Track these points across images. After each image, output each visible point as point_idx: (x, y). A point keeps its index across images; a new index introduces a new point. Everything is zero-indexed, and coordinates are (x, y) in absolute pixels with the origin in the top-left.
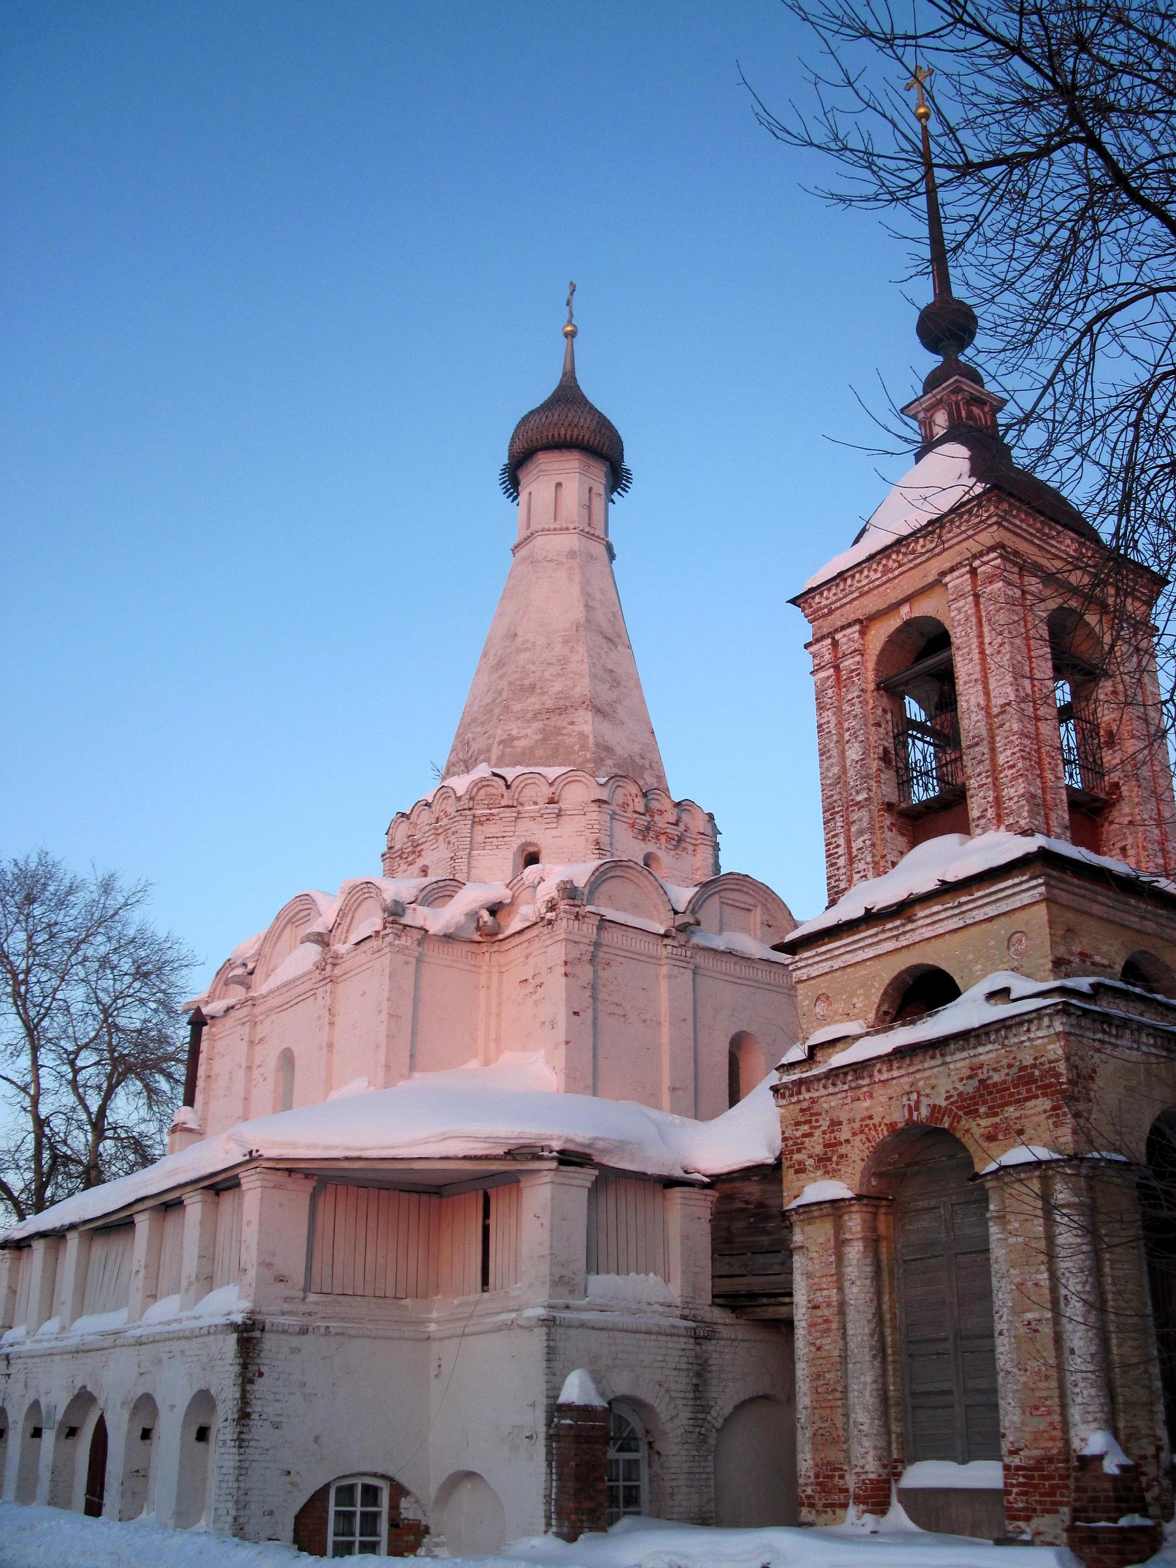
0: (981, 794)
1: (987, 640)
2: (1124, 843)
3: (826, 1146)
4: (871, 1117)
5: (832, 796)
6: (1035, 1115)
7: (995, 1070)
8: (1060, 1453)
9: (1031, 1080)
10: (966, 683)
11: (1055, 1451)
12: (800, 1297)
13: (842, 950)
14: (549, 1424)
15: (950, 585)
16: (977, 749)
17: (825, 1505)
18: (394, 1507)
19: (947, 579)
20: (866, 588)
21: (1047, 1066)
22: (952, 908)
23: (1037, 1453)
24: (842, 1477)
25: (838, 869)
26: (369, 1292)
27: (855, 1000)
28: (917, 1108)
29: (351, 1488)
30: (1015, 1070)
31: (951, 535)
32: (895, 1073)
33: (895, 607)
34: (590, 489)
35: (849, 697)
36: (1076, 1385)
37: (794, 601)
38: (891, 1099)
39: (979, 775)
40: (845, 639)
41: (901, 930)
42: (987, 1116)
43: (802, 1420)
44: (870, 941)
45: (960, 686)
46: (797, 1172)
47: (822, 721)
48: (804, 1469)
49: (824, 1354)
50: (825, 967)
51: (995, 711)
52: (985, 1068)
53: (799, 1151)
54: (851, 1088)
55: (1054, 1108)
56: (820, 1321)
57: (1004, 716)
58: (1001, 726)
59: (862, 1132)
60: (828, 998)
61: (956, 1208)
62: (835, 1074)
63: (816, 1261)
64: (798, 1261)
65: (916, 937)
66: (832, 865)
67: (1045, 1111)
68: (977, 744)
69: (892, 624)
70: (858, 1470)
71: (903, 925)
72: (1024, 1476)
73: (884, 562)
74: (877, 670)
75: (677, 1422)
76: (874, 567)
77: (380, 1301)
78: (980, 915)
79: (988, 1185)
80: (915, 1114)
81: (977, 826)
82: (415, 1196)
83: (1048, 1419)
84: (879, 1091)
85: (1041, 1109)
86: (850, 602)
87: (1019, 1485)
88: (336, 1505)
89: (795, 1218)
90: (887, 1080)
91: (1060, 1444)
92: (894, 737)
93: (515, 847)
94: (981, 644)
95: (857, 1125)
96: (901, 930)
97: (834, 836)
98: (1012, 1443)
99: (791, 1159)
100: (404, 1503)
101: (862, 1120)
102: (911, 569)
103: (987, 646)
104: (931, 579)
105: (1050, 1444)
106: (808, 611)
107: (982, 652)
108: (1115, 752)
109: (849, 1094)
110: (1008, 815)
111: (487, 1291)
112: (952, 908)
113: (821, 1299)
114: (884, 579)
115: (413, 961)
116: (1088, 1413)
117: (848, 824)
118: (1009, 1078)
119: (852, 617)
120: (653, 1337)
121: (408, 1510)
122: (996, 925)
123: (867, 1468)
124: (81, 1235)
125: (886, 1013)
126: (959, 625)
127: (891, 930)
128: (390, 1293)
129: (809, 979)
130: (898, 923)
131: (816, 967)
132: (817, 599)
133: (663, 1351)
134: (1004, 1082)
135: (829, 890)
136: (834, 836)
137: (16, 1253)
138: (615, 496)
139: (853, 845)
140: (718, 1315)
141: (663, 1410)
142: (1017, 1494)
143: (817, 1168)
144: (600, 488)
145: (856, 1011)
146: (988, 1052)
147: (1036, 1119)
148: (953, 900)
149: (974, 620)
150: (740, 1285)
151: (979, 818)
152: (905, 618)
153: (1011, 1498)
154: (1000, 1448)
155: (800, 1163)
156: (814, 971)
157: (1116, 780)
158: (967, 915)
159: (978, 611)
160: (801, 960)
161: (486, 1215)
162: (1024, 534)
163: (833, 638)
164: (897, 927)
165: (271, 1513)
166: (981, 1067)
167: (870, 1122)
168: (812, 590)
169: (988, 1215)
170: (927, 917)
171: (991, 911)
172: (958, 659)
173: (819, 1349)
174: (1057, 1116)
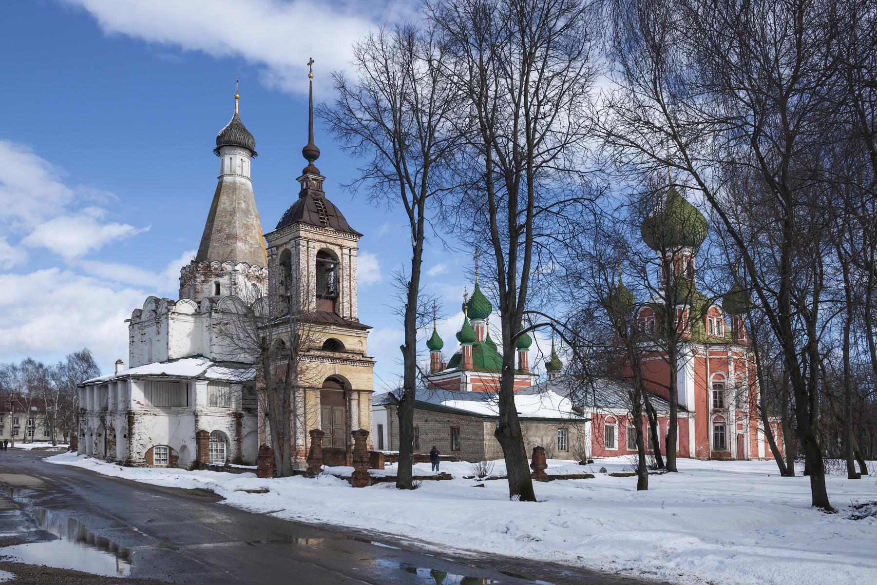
33: (282, 245)
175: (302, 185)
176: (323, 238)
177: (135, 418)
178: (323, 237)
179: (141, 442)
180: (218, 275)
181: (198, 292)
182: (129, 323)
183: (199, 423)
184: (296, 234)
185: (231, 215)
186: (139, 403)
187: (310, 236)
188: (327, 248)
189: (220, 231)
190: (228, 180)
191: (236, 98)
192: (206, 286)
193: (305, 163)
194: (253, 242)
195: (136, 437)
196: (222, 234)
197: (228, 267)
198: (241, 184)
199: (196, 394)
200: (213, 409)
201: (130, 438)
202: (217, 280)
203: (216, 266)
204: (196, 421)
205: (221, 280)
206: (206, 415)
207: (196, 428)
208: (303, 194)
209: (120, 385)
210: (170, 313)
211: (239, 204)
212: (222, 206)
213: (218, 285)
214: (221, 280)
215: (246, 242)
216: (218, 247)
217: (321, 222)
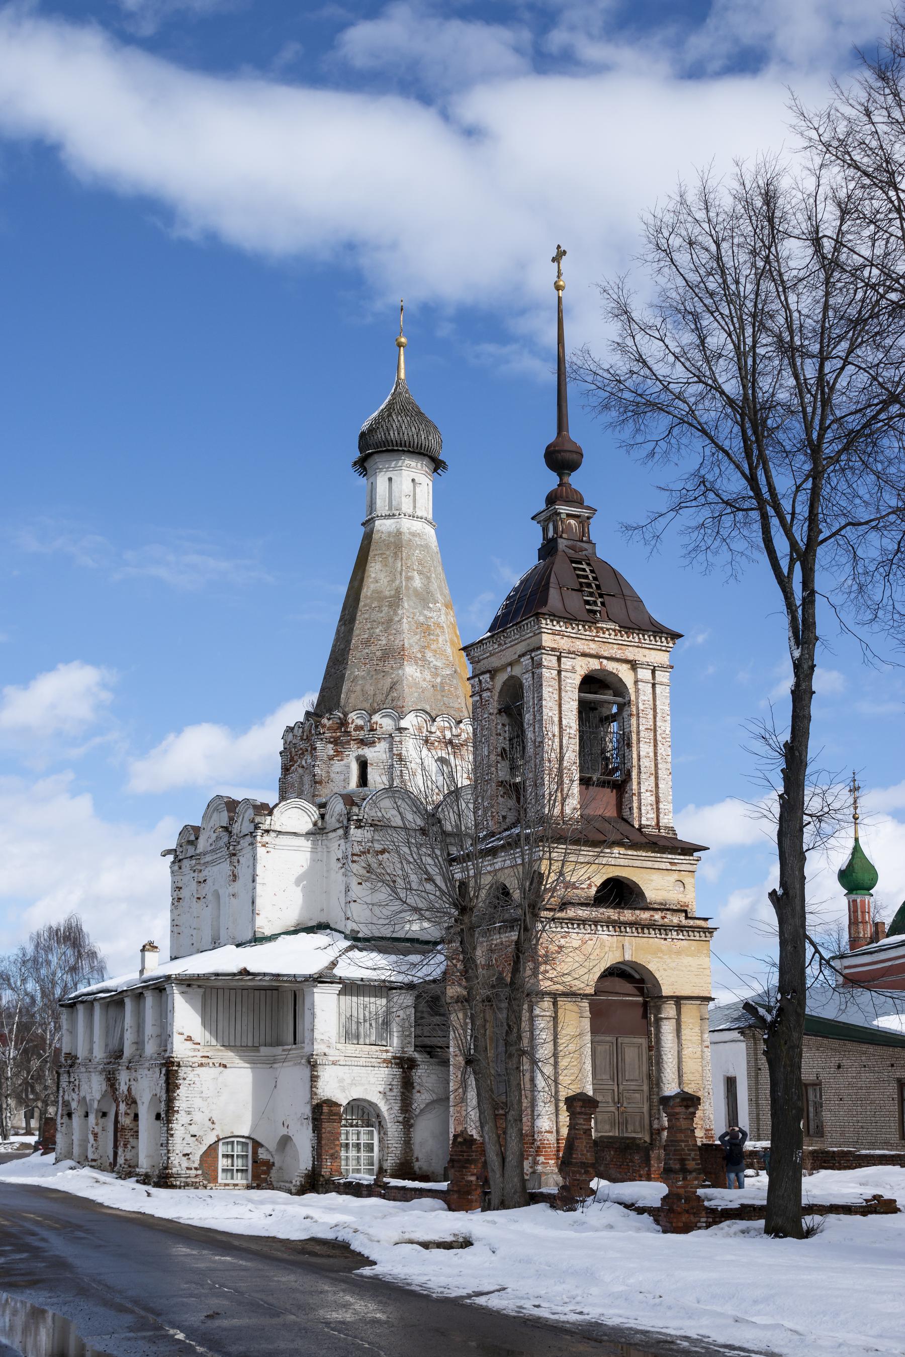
18: (255, 1153)
19: (522, 660)
26: (238, 1044)
33: (503, 668)
34: (413, 480)
74: (499, 701)
100: (260, 1150)
124: (101, 1004)
128: (250, 1044)
138: (439, 471)
140: (417, 1055)
141: (383, 1107)
150: (427, 1041)
175: (545, 530)
176: (592, 648)
177: (181, 1074)
178: (592, 645)
179: (193, 1129)
180: (362, 742)
181: (320, 783)
182: (171, 858)
183: (320, 1083)
184: (533, 642)
185: (390, 606)
186: (189, 1039)
187: (564, 644)
188: (603, 670)
190: (384, 529)
191: (400, 345)
192: (337, 766)
193: (551, 480)
194: (439, 664)
195: (181, 1119)
196: (373, 648)
197: (385, 723)
198: (413, 534)
199: (313, 1015)
200: (351, 1049)
201: (169, 1121)
202: (360, 752)
203: (360, 722)
204: (314, 1079)
205: (369, 753)
208: (548, 550)
209: (150, 999)
210: (259, 832)
211: (409, 579)
212: (372, 586)
213: (363, 765)
214: (369, 753)
215: (423, 662)
216: (363, 678)
217: (590, 611)
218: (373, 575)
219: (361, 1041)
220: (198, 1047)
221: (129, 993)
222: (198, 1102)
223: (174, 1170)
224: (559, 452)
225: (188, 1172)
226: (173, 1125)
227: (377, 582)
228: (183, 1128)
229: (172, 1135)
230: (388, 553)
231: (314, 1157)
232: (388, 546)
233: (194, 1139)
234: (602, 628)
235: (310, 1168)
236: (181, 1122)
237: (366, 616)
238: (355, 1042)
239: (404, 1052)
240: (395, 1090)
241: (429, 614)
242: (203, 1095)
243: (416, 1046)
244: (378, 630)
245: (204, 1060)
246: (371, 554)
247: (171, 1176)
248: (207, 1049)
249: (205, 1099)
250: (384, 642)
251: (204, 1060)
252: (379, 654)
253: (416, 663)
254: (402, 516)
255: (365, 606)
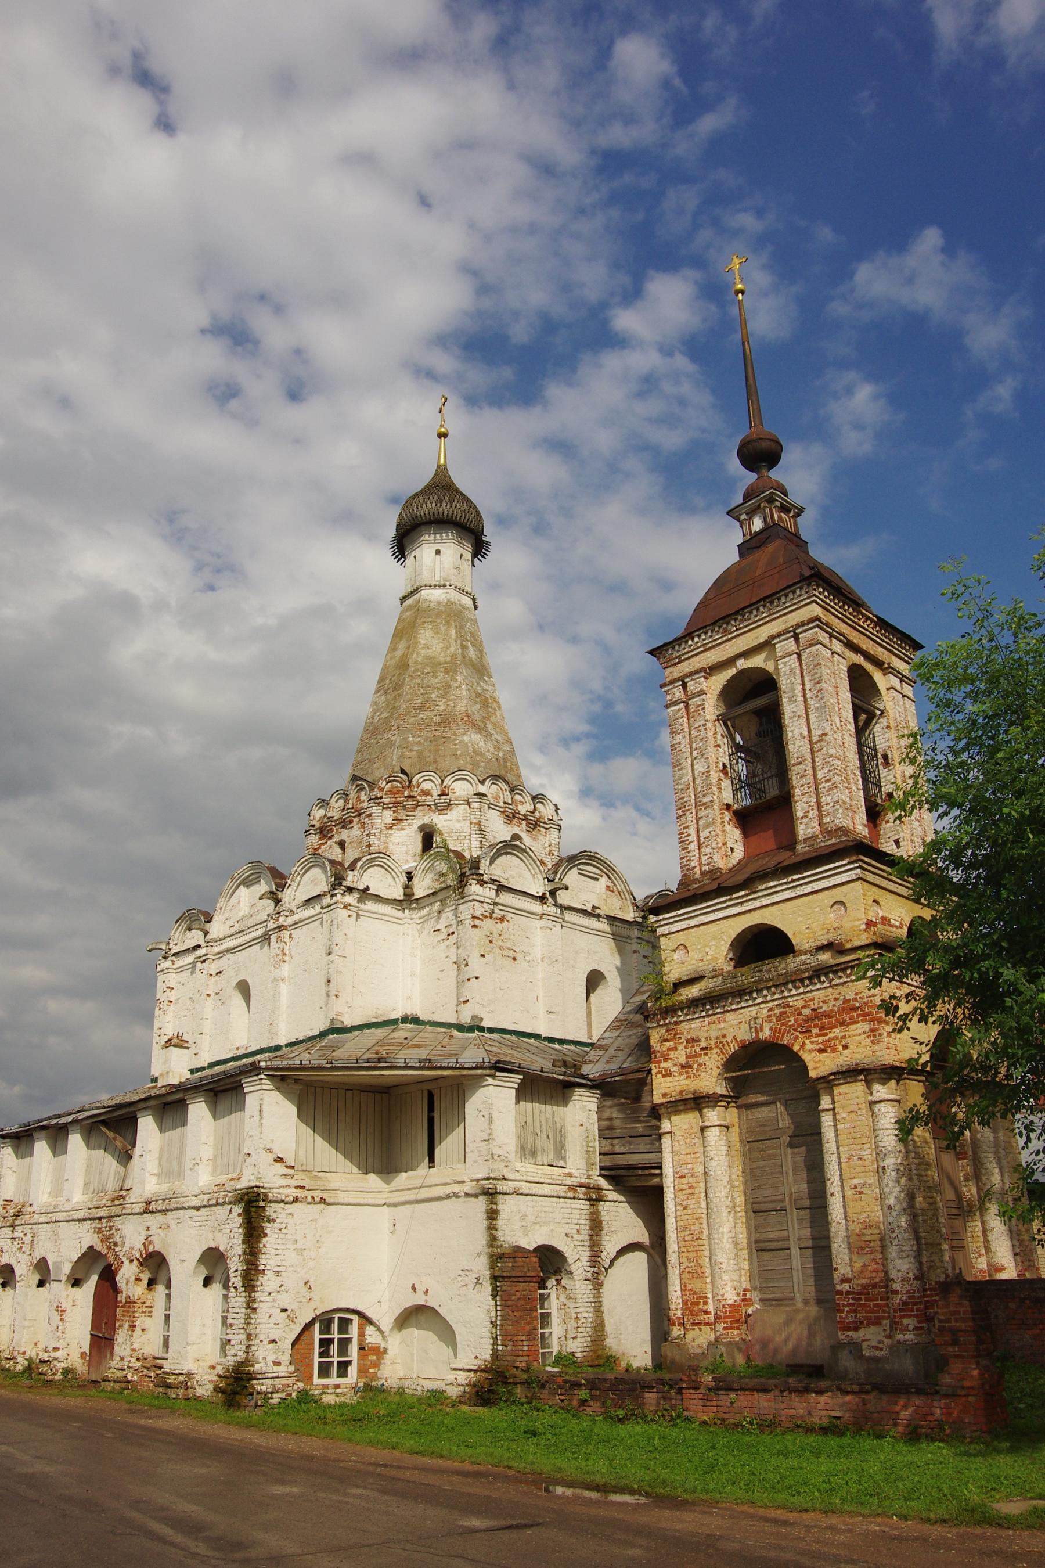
0: (804, 800)
1: (807, 687)
2: (898, 837)
3: (687, 1058)
4: (724, 1036)
5: (683, 798)
6: (856, 1035)
7: (824, 1002)
8: (881, 1281)
9: (854, 1009)
10: (790, 718)
11: (877, 1280)
12: (668, 1170)
13: (698, 913)
14: (492, 1267)
15: (777, 646)
16: (800, 766)
17: (693, 1324)
18: (362, 1335)
20: (710, 645)
21: (865, 1000)
22: (786, 883)
23: (864, 1281)
24: (706, 1303)
25: (689, 852)
27: (707, 949)
28: (762, 1030)
29: (330, 1321)
30: (838, 1003)
31: (779, 609)
32: (743, 1004)
34: (462, 556)
35: (697, 725)
36: (893, 1232)
37: (652, 652)
38: (740, 1022)
39: (802, 786)
40: (692, 683)
41: (745, 899)
42: (818, 1035)
43: (672, 1262)
44: (720, 906)
45: (787, 720)
46: (664, 1076)
47: (675, 742)
48: (674, 1298)
49: (690, 1211)
50: (684, 925)
51: (815, 739)
52: (816, 1002)
53: (666, 1060)
54: (709, 1016)
55: (871, 1030)
56: (686, 1187)
57: (822, 743)
58: (820, 750)
59: (717, 1047)
60: (686, 947)
61: (789, 1103)
62: (695, 1004)
63: (682, 1142)
64: (666, 1141)
65: (757, 904)
66: (684, 849)
67: (865, 1033)
68: (800, 763)
69: (731, 672)
70: (719, 1297)
71: (747, 895)
72: (853, 1299)
73: (725, 626)
75: (578, 1264)
76: (716, 629)
77: (348, 1176)
78: (808, 889)
79: (819, 1086)
80: (761, 1034)
81: (801, 823)
82: (372, 1095)
83: (872, 1256)
84: (730, 1017)
85: (862, 1031)
86: (696, 655)
87: (849, 1305)
88: (321, 1333)
89: (662, 1111)
90: (738, 1009)
91: (882, 1275)
92: (729, 755)
93: (415, 827)
94: (804, 689)
95: (712, 1042)
96: (745, 899)
97: (684, 828)
98: (843, 1275)
99: (659, 1067)
100: (370, 1330)
101: (717, 1038)
102: (745, 632)
103: (807, 692)
104: (761, 640)
105: (874, 1275)
106: (662, 660)
107: (804, 696)
108: (889, 771)
109: (706, 1019)
110: (826, 816)
111: (434, 1167)
112: (786, 883)
113: (686, 1171)
114: (724, 639)
115: (354, 915)
116: (902, 1251)
117: (698, 819)
118: (836, 1008)
119: (698, 666)
120: (562, 1200)
121: (372, 1337)
122: (820, 895)
123: (726, 1296)
125: (731, 959)
126: (785, 675)
127: (737, 898)
129: (670, 933)
130: (743, 893)
131: (676, 924)
132: (670, 652)
133: (569, 1211)
134: (832, 1010)
135: (681, 867)
136: (684, 828)
137: (16, 1140)
139: (701, 835)
140: (603, 1183)
142: (847, 1312)
143: (681, 1074)
144: (468, 555)
145: (709, 958)
146: (818, 990)
147: (858, 1038)
148: (786, 877)
149: (798, 672)
150: (622, 1160)
151: (802, 818)
152: (740, 668)
153: (843, 1315)
154: (832, 1279)
155: (666, 1070)
156: (674, 928)
157: (890, 790)
158: (798, 889)
159: (801, 665)
160: (664, 919)
161: (431, 1109)
162: (832, 610)
163: (683, 681)
164: (742, 897)
165: (274, 1341)
166: (813, 999)
167: (724, 1040)
168: (666, 645)
169: (820, 1108)
170: (766, 889)
171: (817, 886)
172: (784, 700)
173: (685, 1208)
174: (874, 1036)
179: (284, 1300)
185: (447, 672)
186: (279, 1160)
189: (422, 707)
194: (499, 738)
195: (267, 1282)
204: (492, 1215)
206: (516, 1193)
207: (493, 1239)
218: (423, 642)
219: (539, 1160)
220: (291, 1171)
221: (152, 1103)
222: (291, 1257)
223: (257, 1367)
224: (754, 441)
225: (276, 1369)
226: (257, 1295)
227: (428, 648)
228: (269, 1298)
229: (254, 1310)
230: (439, 621)
231: (495, 1339)
232: (438, 615)
233: (284, 1315)
234: (863, 615)
235: (488, 1357)
236: (268, 1289)
237: (419, 681)
238: (532, 1161)
239: (589, 1177)
240: (583, 1232)
241: (486, 687)
242: (299, 1246)
243: (602, 1168)
244: (433, 696)
245: (300, 1193)
246: (420, 622)
247: (251, 1377)
248: (301, 1175)
249: (300, 1251)
250: (442, 708)
251: (300, 1193)
252: (437, 719)
253: (480, 733)
254: (453, 587)
255: (416, 670)
